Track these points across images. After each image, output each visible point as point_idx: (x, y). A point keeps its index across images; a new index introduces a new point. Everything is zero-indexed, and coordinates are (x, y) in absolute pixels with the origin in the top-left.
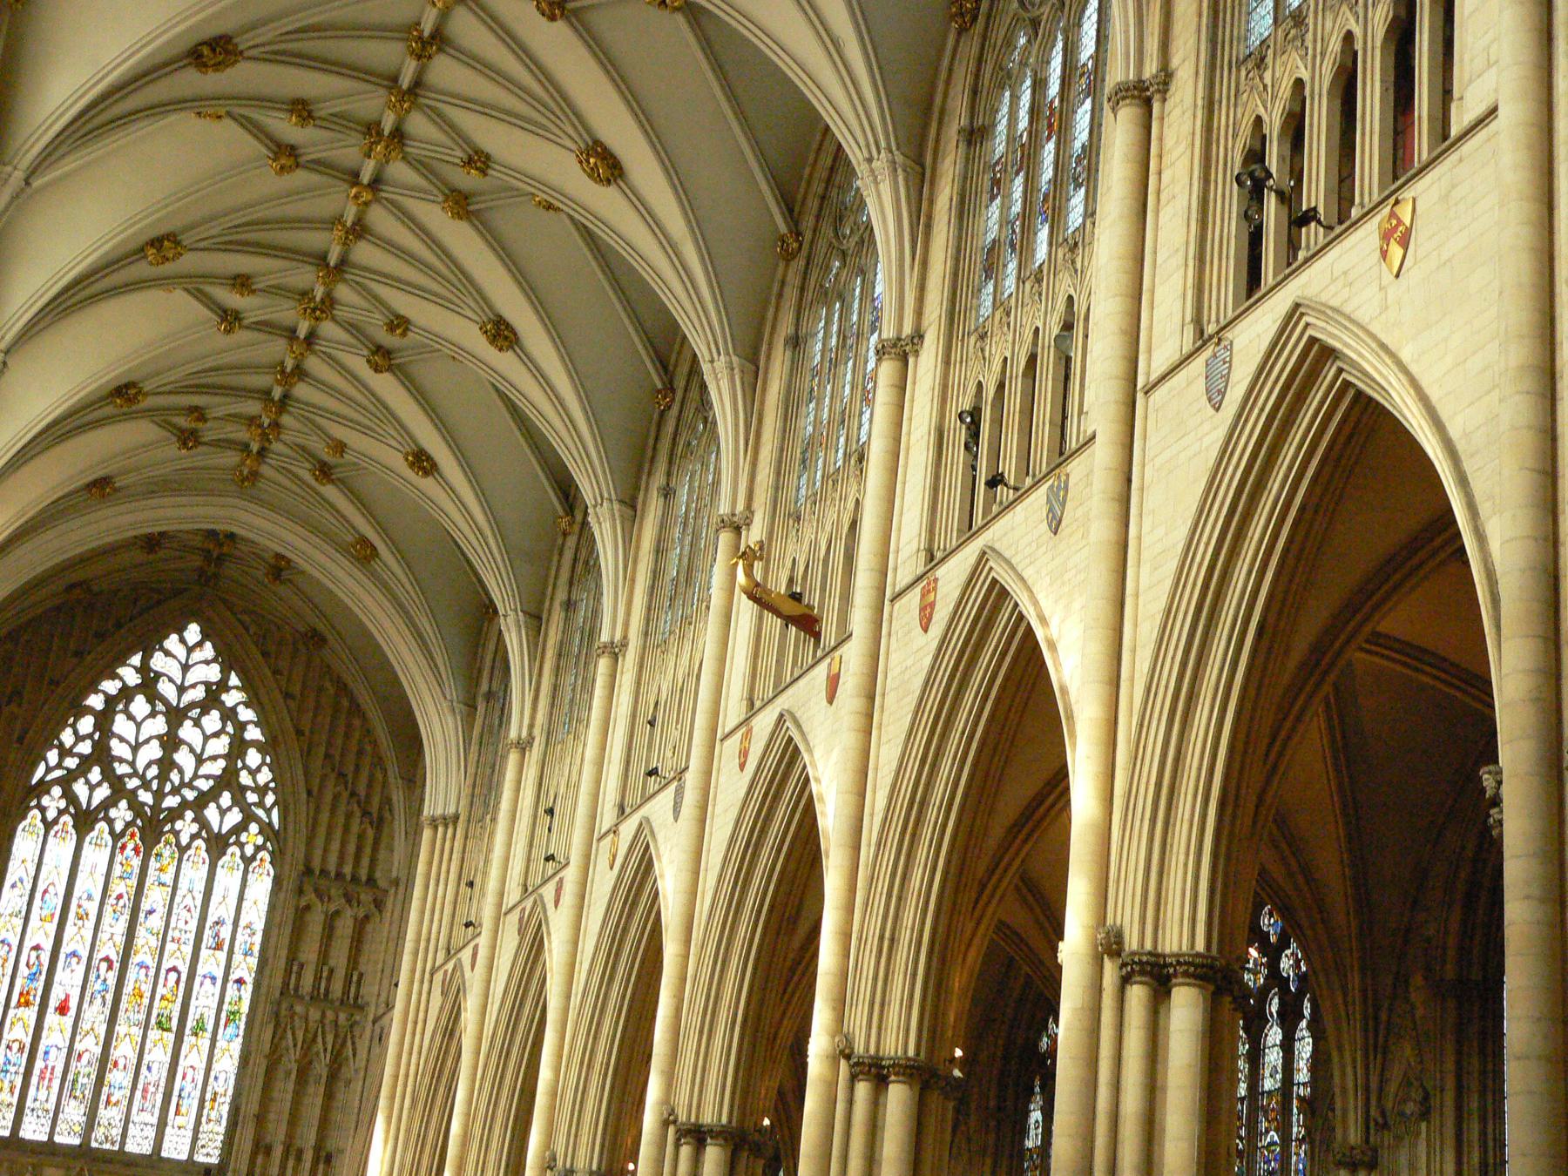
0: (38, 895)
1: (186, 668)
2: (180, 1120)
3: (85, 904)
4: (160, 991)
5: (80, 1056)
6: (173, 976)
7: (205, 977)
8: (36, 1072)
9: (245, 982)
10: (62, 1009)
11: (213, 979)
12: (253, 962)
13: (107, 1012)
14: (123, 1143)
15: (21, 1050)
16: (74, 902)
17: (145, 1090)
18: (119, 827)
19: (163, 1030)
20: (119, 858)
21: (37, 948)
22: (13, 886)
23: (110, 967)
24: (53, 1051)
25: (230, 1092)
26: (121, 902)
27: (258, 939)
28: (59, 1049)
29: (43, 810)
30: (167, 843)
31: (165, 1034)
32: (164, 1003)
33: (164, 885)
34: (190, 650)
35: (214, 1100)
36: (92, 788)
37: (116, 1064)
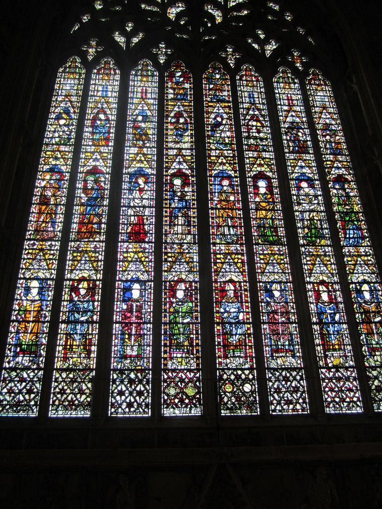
0: (88, 123)
2: (335, 359)
3: (143, 125)
5: (173, 291)
6: (262, 184)
9: (346, 181)
10: (137, 235)
13: (194, 230)
14: (265, 404)
15: (91, 290)
16: (129, 124)
17: (273, 323)
18: (162, 60)
19: (272, 243)
21: (94, 171)
22: (59, 117)
23: (185, 183)
26: (182, 120)
27: (340, 137)
29: (83, 55)
30: (214, 68)
31: (276, 249)
33: (223, 101)
35: (368, 321)
36: (128, 36)
37: (223, 291)
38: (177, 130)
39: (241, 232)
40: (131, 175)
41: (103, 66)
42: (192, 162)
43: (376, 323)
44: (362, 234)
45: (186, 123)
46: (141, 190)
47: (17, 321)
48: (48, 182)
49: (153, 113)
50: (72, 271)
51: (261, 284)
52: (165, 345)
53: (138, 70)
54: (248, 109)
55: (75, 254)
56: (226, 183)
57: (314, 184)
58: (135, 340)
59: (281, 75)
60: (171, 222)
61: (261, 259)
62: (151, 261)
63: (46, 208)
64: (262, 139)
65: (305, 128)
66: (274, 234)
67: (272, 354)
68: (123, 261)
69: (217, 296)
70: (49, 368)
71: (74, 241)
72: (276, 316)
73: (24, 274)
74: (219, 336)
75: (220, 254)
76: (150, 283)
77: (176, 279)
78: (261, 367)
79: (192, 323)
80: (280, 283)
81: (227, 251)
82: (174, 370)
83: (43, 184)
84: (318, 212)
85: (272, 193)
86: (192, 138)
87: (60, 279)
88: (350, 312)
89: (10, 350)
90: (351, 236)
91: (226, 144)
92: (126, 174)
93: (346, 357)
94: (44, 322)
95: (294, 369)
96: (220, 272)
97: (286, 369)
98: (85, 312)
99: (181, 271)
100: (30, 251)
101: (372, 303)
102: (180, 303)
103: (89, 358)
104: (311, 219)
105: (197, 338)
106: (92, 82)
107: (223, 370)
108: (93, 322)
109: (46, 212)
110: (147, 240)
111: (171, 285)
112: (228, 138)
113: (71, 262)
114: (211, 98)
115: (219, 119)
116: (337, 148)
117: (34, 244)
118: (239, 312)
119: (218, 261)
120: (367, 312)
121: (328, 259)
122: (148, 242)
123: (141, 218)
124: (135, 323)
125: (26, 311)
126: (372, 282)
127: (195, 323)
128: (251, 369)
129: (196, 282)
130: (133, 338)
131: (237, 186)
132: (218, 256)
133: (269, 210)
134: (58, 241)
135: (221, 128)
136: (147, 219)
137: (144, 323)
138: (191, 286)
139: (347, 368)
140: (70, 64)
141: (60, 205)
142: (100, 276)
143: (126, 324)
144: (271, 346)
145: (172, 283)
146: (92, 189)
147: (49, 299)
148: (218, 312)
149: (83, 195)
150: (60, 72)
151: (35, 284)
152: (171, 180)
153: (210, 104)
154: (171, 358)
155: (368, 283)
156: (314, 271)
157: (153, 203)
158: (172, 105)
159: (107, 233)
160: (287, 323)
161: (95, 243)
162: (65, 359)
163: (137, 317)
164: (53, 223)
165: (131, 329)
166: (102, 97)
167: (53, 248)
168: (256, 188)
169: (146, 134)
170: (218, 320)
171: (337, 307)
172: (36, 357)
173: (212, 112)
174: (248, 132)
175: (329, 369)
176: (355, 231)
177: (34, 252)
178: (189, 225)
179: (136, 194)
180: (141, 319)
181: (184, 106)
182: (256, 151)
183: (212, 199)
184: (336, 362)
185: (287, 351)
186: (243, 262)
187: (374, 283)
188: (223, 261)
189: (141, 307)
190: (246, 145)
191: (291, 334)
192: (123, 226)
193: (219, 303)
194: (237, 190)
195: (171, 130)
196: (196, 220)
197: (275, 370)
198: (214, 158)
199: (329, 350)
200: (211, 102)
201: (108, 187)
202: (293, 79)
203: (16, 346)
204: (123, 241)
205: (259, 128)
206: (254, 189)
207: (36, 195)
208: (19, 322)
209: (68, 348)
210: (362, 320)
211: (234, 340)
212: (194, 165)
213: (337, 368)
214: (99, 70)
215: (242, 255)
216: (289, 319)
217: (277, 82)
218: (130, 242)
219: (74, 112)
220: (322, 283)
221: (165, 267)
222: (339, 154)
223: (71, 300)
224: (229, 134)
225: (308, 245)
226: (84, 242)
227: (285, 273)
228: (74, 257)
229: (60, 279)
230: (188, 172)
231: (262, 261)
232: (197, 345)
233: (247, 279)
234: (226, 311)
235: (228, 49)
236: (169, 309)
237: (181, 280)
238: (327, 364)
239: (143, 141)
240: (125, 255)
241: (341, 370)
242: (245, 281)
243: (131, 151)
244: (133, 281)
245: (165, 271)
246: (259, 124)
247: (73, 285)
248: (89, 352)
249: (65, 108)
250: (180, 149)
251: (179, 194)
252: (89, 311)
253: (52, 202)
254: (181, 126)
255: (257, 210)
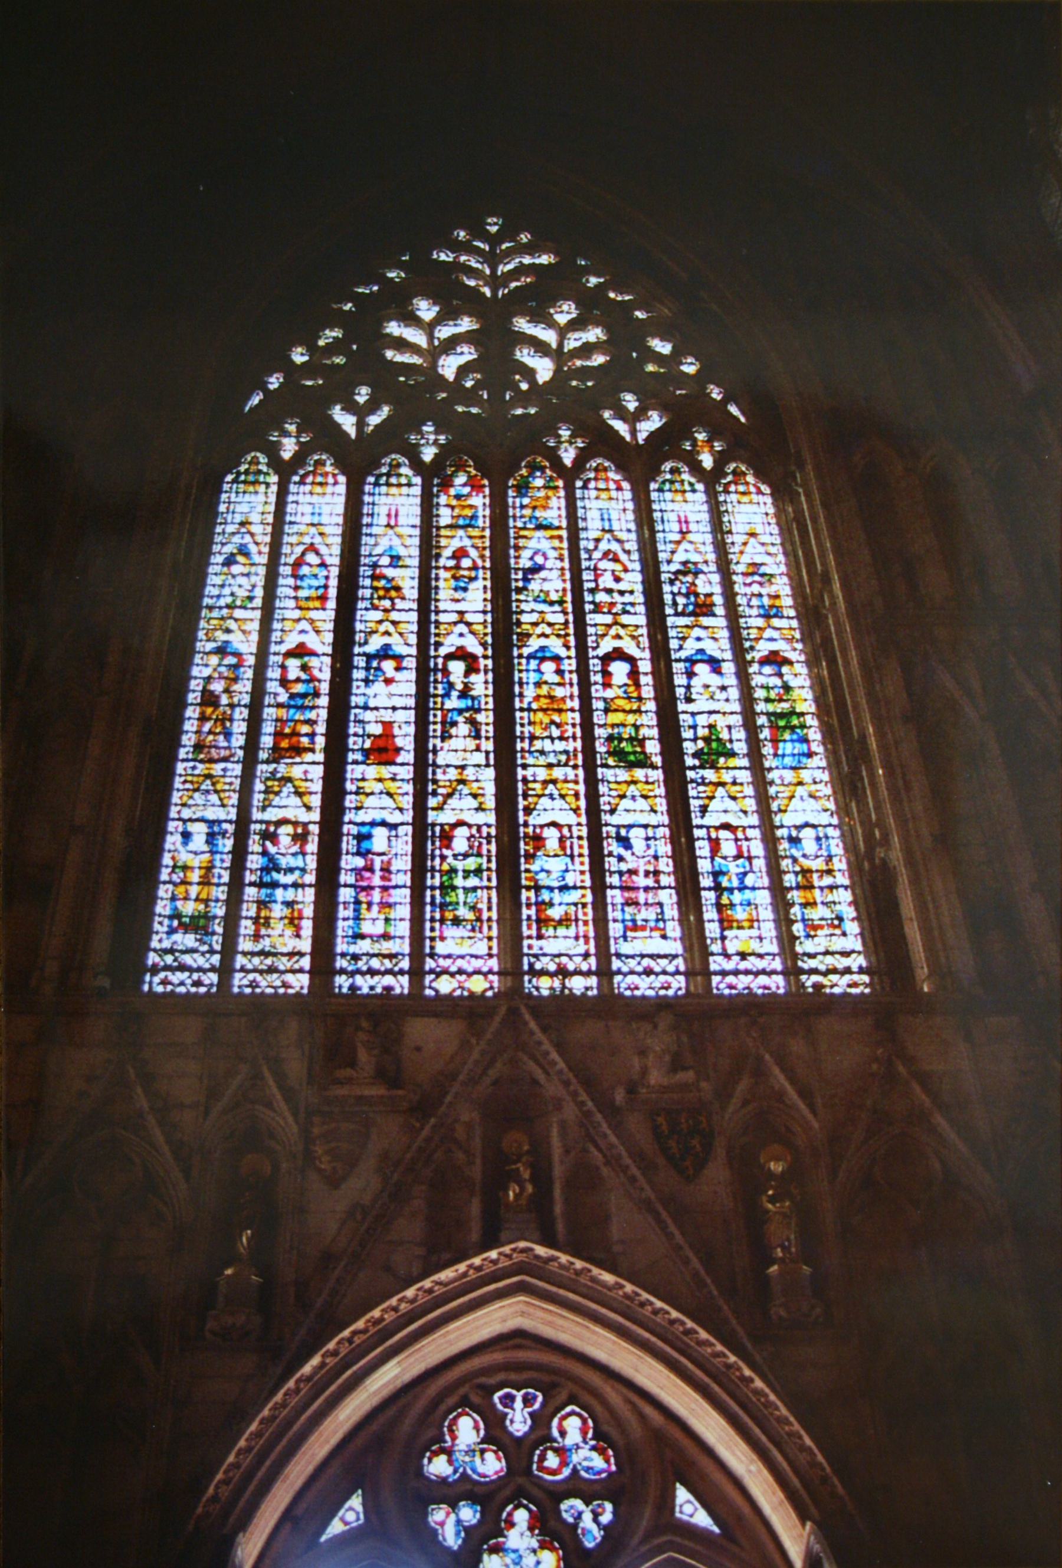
1: (492, 259)
3: (390, 572)
4: (597, 691)
5: (447, 838)
7: (691, 661)
8: (345, 878)
11: (715, 665)
12: (789, 623)
20: (443, 499)
21: (301, 651)
23: (472, 668)
24: (380, 833)
25: (840, 864)
26: (466, 563)
27: (782, 586)
28: (394, 827)
29: (273, 451)
30: (533, 468)
31: (639, 773)
32: (615, 718)
34: (494, 240)
36: (361, 413)
37: (538, 841)
38: (455, 578)
39: (575, 750)
40: (369, 657)
41: (311, 469)
42: (486, 634)
43: (821, 888)
44: (809, 749)
45: (475, 568)
46: (388, 681)
47: (170, 882)
48: (215, 670)
49: (411, 553)
50: (264, 809)
51: (609, 828)
52: (433, 920)
53: (382, 475)
54: (597, 540)
55: (269, 783)
56: (549, 667)
57: (720, 667)
58: (379, 912)
59: (668, 476)
60: (443, 731)
61: (611, 790)
62: (407, 794)
63: (213, 712)
64: (622, 593)
65: (710, 572)
66: (638, 749)
67: (625, 932)
68: (357, 793)
69: (527, 848)
70: (229, 949)
71: (267, 762)
72: (634, 877)
73: (179, 812)
74: (529, 906)
75: (535, 781)
76: (405, 827)
77: (453, 821)
78: (604, 953)
79: (482, 888)
80: (646, 826)
81: (548, 778)
82: (449, 956)
83: (207, 672)
84: (724, 713)
85: (637, 685)
86: (485, 592)
87: (243, 822)
88: (775, 872)
89: (161, 923)
90: (788, 751)
91: (552, 603)
92: (359, 655)
93: (761, 938)
94: (218, 885)
95: (665, 956)
96: (534, 809)
97: (651, 956)
98: (291, 870)
99: (460, 808)
100: (189, 778)
101: (817, 857)
102: (460, 858)
103: (298, 936)
104: (711, 727)
105: (490, 909)
106: (291, 498)
107: (536, 956)
108: (303, 886)
109: (214, 717)
110: (399, 760)
111: (442, 830)
112: (557, 591)
113: (262, 796)
114: (525, 523)
115: (539, 559)
116: (772, 607)
117: (194, 768)
118: (567, 871)
119: (531, 792)
120: (806, 872)
121: (738, 788)
122: (402, 764)
123: (388, 725)
124: (380, 887)
125: (185, 868)
126: (820, 826)
127: (489, 888)
128: (586, 956)
129: (489, 826)
130: (375, 908)
131: (571, 672)
132: (531, 785)
133: (631, 711)
134: (237, 762)
135: (543, 574)
136: (400, 727)
137: (396, 887)
138: (479, 830)
139: (761, 956)
140: (247, 466)
141: (239, 705)
142: (316, 816)
143: (364, 889)
144: (623, 921)
145: (446, 827)
146: (298, 680)
147: (226, 850)
148: (527, 871)
149: (281, 690)
150: (228, 483)
151: (199, 830)
152: (445, 664)
153: (523, 533)
154: (442, 938)
155: (814, 826)
156: (709, 809)
157: (412, 702)
158: (447, 537)
159: (326, 750)
160: (654, 888)
161: (305, 767)
162: (257, 937)
163: (383, 878)
164: (228, 735)
165: (371, 896)
166: (313, 525)
167: (229, 773)
168: (606, 674)
169: (398, 589)
170: (528, 883)
171: (751, 864)
172: (207, 934)
173: (525, 548)
174: (596, 581)
175: (727, 956)
176: (797, 745)
177: (195, 779)
178: (478, 736)
179: (379, 687)
180: (390, 880)
181: (470, 537)
182: (609, 612)
183: (521, 695)
184: (742, 948)
185: (652, 930)
186: (577, 795)
187: (825, 826)
188: (540, 792)
189: (389, 862)
190: (590, 603)
191: (660, 905)
192: (356, 738)
193: (530, 857)
194: (571, 679)
195: (446, 580)
196: (491, 728)
197: (628, 957)
198: (528, 627)
199: (731, 928)
200: (525, 528)
201: (326, 675)
202: (691, 484)
203: (171, 917)
204: (355, 762)
205: (617, 573)
206: (603, 677)
207: (194, 691)
208: (175, 885)
209: (261, 922)
210: (798, 883)
211: (555, 913)
212: (489, 639)
213: (743, 956)
214: (303, 477)
215: (576, 782)
216: (657, 881)
217: (660, 490)
218: (368, 765)
219: (260, 553)
220: (726, 826)
221: (432, 802)
222: (776, 616)
223: (265, 853)
224: (560, 585)
225: (702, 767)
226: (286, 764)
227: (655, 812)
228: (267, 787)
229: (243, 822)
230: (478, 651)
231: (614, 793)
232: (489, 919)
233: (583, 820)
234: (542, 870)
235: (561, 432)
236: (441, 865)
237: (461, 823)
238: (724, 949)
239: (392, 599)
240: (361, 784)
241: (752, 959)
242: (579, 824)
243: (366, 617)
244: (373, 824)
245: (433, 809)
246: (618, 567)
247: (267, 829)
248: (298, 928)
249: (241, 545)
250: (461, 613)
251: (459, 686)
252: (297, 868)
253: (224, 700)
254: (466, 573)
255: (607, 711)
